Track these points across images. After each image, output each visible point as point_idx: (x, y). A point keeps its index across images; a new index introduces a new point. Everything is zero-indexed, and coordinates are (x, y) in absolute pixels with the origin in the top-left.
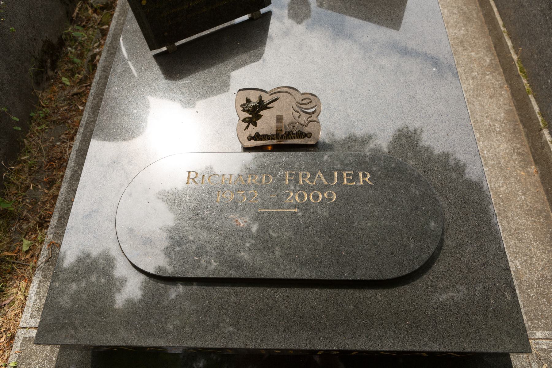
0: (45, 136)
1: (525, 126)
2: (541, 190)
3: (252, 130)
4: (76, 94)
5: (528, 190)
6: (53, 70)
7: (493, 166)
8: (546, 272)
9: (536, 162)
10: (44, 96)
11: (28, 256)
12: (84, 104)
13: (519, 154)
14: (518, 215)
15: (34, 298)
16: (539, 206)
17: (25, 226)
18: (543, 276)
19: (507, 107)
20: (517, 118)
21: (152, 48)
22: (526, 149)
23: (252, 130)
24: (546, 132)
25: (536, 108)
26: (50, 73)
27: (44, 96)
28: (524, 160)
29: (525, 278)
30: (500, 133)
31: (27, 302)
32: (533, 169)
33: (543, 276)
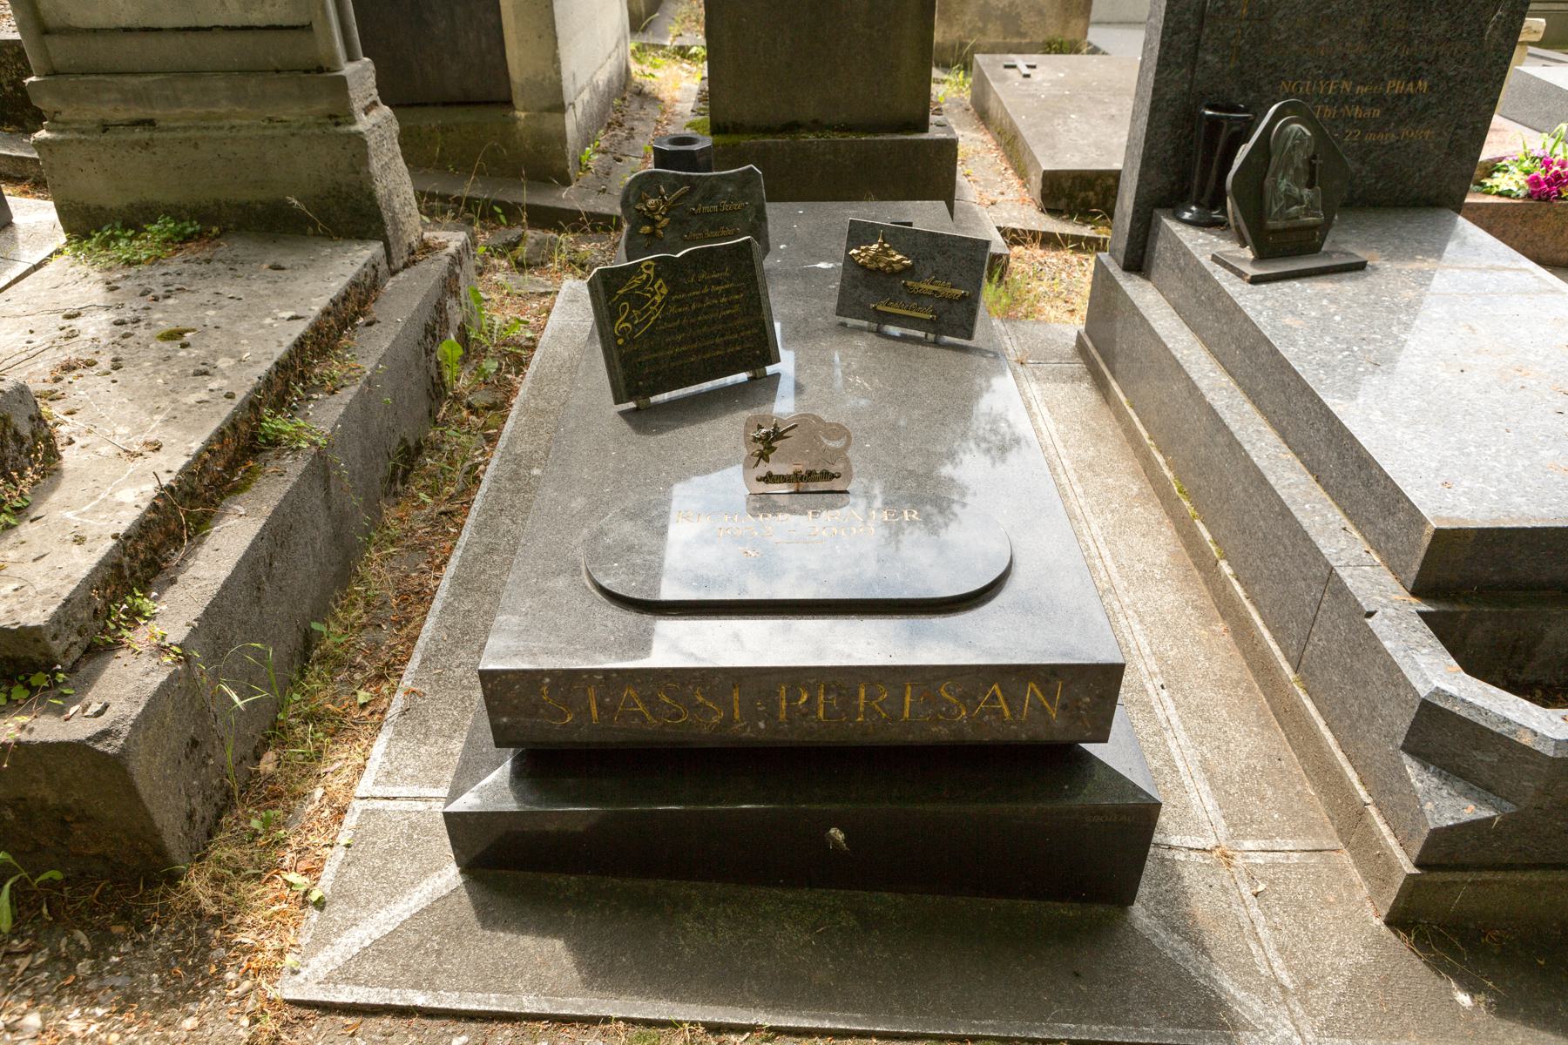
0: (392, 563)
1: (1200, 570)
2: (1237, 654)
3: (762, 469)
4: (444, 513)
5: (1214, 653)
6: (403, 484)
7: (1153, 623)
8: (1253, 762)
9: (1224, 615)
10: (391, 514)
11: (366, 713)
12: (460, 526)
13: (1195, 608)
14: (1200, 686)
15: (380, 760)
16: (1235, 675)
17: (358, 676)
18: (1248, 766)
19: (1171, 548)
20: (1189, 561)
21: (617, 401)
22: (1208, 602)
23: (762, 469)
24: (1223, 564)
25: (1207, 536)
26: (399, 487)
27: (391, 514)
28: (1204, 615)
29: (1219, 770)
30: (1162, 581)
31: (368, 764)
32: (1220, 626)
33: (1248, 766)
